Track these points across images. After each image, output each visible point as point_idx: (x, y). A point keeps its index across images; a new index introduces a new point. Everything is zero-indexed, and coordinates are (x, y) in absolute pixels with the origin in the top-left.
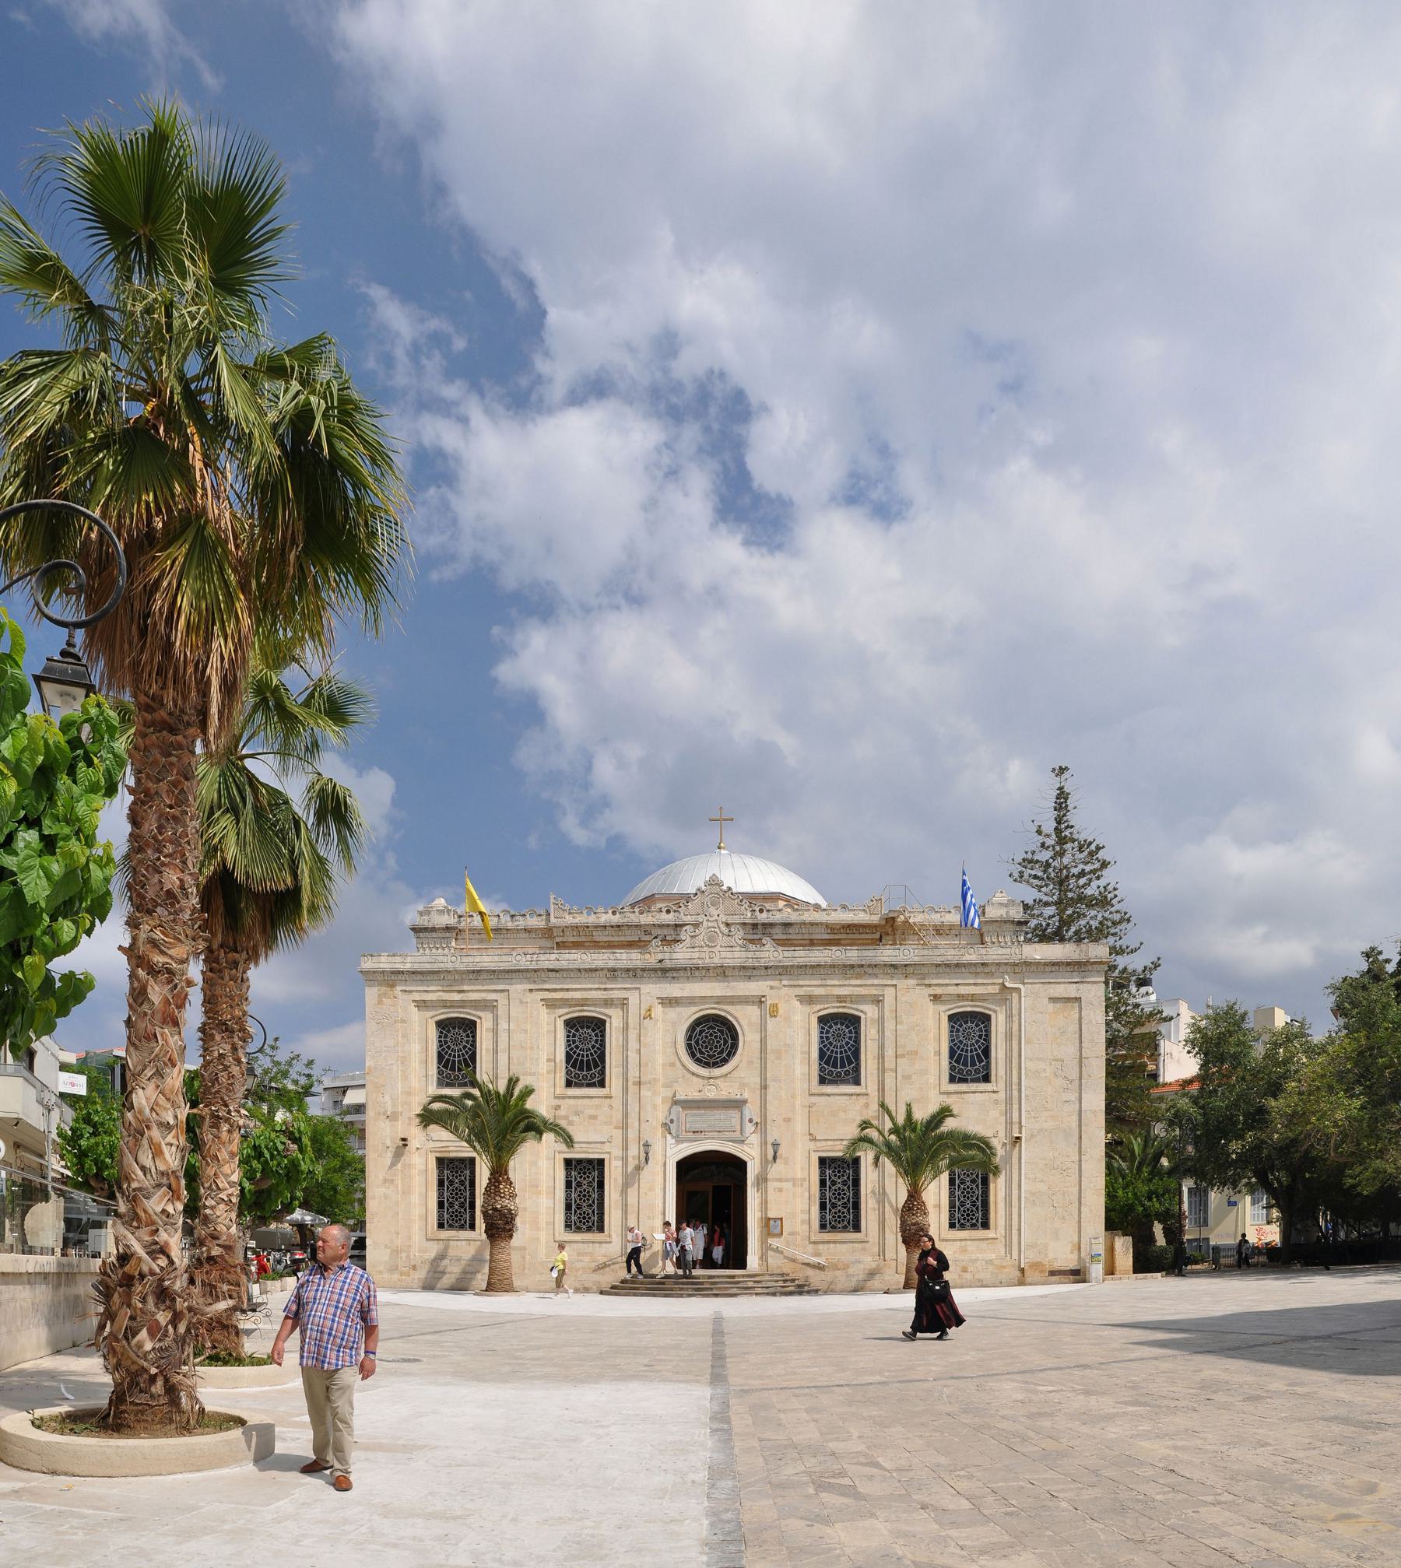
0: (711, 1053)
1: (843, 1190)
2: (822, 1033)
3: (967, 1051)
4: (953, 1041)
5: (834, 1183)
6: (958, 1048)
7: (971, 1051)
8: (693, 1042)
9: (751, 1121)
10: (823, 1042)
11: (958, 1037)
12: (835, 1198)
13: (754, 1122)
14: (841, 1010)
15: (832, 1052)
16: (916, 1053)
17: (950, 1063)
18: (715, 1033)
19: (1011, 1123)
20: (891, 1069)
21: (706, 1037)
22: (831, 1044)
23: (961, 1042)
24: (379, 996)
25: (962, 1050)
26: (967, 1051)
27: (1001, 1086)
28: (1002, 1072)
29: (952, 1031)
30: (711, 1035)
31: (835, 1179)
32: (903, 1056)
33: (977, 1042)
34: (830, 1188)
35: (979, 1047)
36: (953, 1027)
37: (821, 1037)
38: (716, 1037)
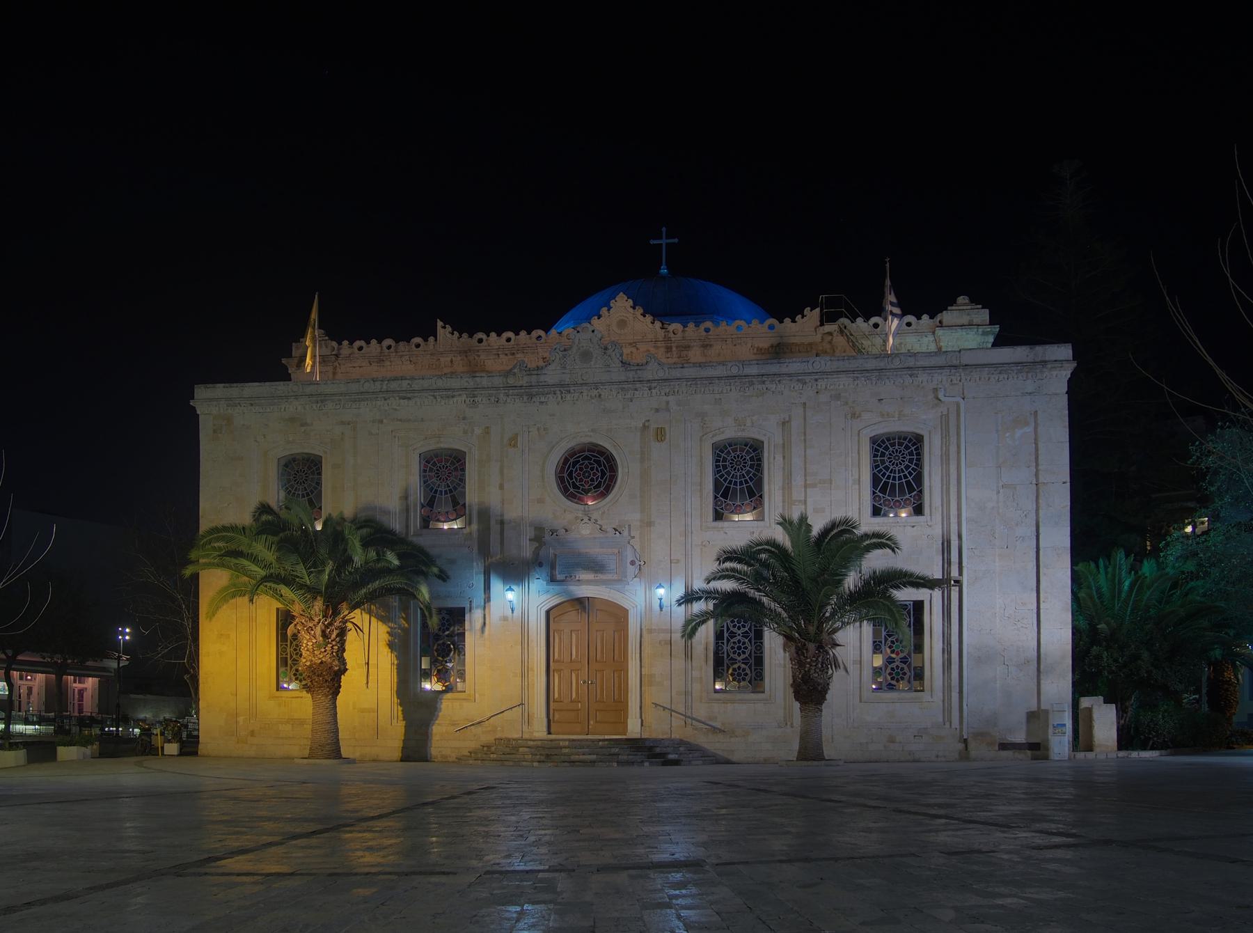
0: (587, 487)
1: (744, 643)
2: (717, 461)
3: (894, 478)
4: (877, 466)
5: (732, 635)
6: (884, 475)
7: (900, 478)
8: (565, 475)
9: (633, 563)
10: (719, 472)
11: (883, 462)
12: (734, 653)
13: (637, 563)
14: (740, 434)
15: (730, 482)
16: (831, 480)
17: (874, 493)
18: (591, 464)
19: (949, 563)
20: (800, 501)
21: (581, 469)
22: (728, 473)
23: (887, 468)
24: (215, 431)
25: (889, 477)
26: (894, 478)
27: (938, 517)
28: (937, 501)
29: (875, 456)
30: (587, 467)
31: (735, 630)
32: (814, 486)
33: (907, 467)
34: (728, 641)
35: (910, 474)
36: (877, 450)
37: (717, 466)
38: (592, 469)
